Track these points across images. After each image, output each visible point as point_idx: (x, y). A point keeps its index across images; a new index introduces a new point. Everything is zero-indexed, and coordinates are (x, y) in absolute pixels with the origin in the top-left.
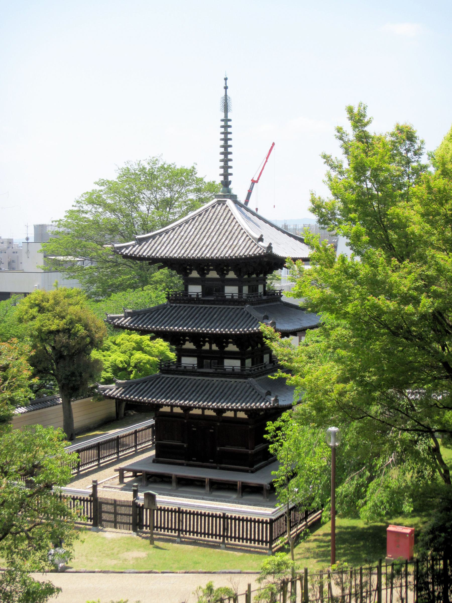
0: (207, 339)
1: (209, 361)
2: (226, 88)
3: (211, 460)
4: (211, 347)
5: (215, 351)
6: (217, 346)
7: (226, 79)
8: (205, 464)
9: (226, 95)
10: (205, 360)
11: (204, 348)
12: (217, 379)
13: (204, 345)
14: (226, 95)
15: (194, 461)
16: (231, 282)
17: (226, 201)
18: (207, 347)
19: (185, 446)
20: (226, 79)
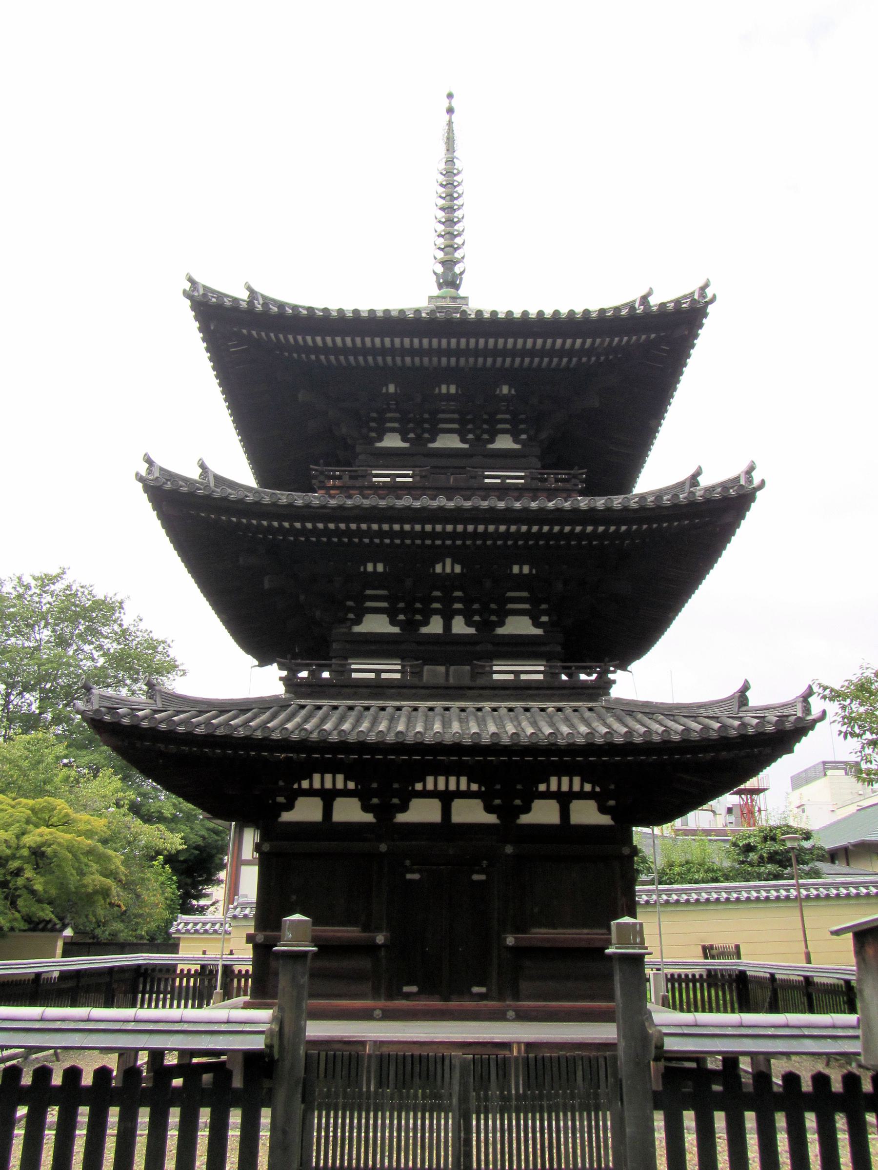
1: (442, 669)
2: (450, 111)
3: (476, 989)
4: (447, 626)
5: (462, 639)
6: (469, 623)
7: (450, 96)
8: (453, 1004)
9: (450, 123)
10: (426, 668)
11: (424, 630)
12: (494, 704)
13: (426, 623)
14: (450, 123)
15: (408, 996)
18: (435, 626)
19: (380, 939)
20: (450, 96)
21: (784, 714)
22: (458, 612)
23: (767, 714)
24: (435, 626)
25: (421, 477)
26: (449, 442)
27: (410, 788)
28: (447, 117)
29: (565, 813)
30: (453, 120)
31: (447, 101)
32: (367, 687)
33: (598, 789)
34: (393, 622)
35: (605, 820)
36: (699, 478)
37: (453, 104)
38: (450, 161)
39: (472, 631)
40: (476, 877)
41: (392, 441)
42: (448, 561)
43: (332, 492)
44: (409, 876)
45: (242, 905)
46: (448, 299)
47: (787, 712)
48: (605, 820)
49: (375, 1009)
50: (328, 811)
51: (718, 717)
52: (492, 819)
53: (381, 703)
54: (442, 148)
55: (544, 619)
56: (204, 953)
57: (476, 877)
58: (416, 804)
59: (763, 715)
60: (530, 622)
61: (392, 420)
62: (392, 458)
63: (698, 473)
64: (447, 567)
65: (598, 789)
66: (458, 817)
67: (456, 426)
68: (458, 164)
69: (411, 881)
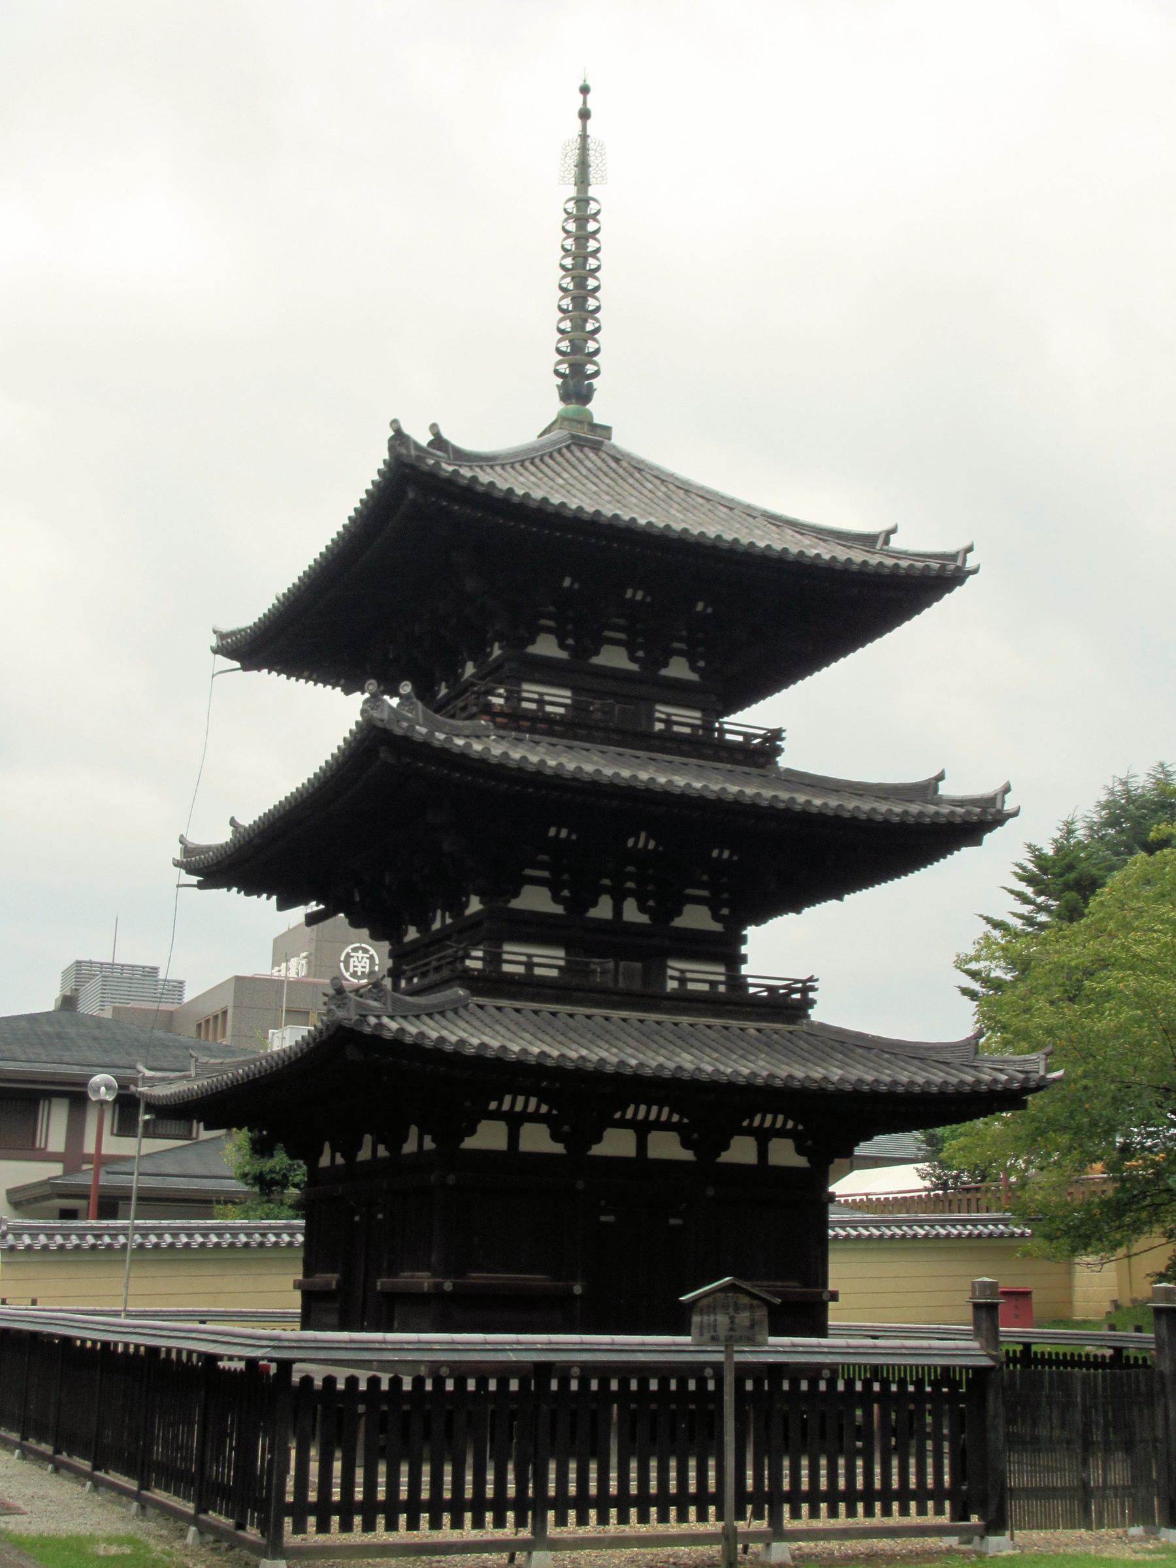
0: (606, 882)
1: (611, 965)
2: (585, 115)
4: (618, 910)
6: (642, 909)
7: (585, 90)
9: (584, 137)
11: (593, 913)
12: (692, 1020)
13: (594, 904)
14: (584, 137)
16: (679, 693)
17: (601, 443)
18: (603, 910)
19: (578, 1289)
20: (585, 90)
21: (1026, 1069)
23: (1005, 1067)
24: (603, 910)
25: (604, 713)
26: (613, 658)
28: (579, 122)
29: (763, 1152)
30: (588, 133)
31: (581, 97)
32: (551, 988)
33: (800, 1127)
34: (556, 899)
35: (802, 1162)
36: (940, 784)
37: (589, 106)
38: (582, 201)
39: (644, 919)
40: (673, 1222)
41: (546, 647)
42: (643, 835)
43: (499, 720)
44: (603, 1218)
45: (14, 1229)
46: (586, 428)
47: (1028, 1068)
48: (802, 1162)
49: (572, 1367)
50: (513, 1138)
51: (948, 1063)
52: (687, 1155)
53: (569, 1009)
54: (572, 173)
56: (34, 1302)
57: (673, 1222)
58: (610, 1133)
59: (1001, 1067)
60: (709, 913)
61: (548, 616)
62: (547, 671)
63: (941, 777)
64: (643, 841)
65: (800, 1127)
66: (653, 1153)
67: (622, 636)
68: (593, 208)
69: (606, 1223)
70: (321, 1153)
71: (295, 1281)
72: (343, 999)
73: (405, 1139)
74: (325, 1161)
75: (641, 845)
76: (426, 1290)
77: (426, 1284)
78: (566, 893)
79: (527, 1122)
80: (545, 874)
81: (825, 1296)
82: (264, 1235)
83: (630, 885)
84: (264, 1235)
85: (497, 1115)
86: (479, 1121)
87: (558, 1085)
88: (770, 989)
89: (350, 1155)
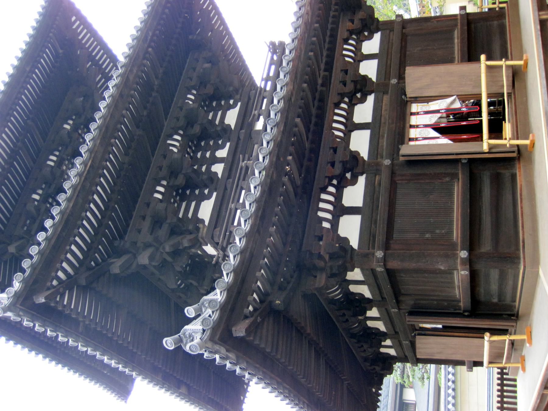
4: (221, 160)
5: (233, 153)
6: (222, 147)
13: (216, 174)
22: (213, 155)
27: (338, 140)
34: (209, 197)
42: (169, 142)
48: (377, 37)
55: (231, 102)
70: (388, 355)
71: (468, 371)
72: (186, 337)
73: (362, 295)
74: (392, 352)
75: (177, 144)
76: (467, 273)
77: (463, 272)
78: (206, 192)
79: (342, 202)
80: (193, 204)
81: (463, 12)
82: (449, 380)
83: (208, 154)
84: (449, 380)
85: (335, 224)
86: (339, 235)
87: (290, 158)
88: (270, 65)
89: (384, 336)
